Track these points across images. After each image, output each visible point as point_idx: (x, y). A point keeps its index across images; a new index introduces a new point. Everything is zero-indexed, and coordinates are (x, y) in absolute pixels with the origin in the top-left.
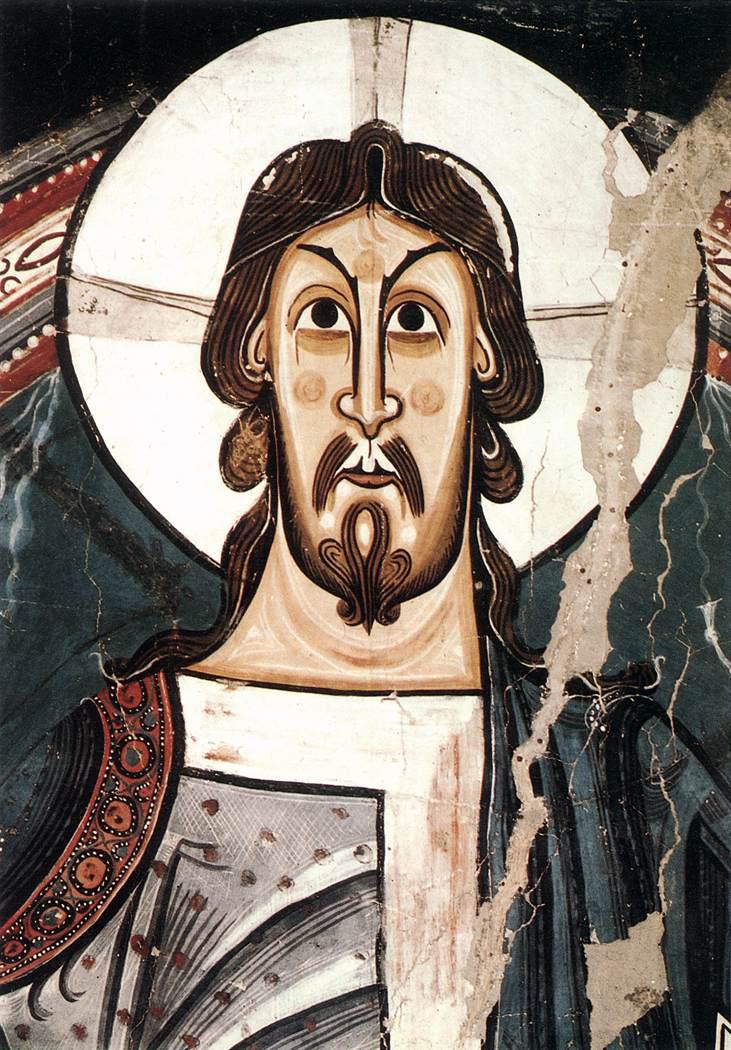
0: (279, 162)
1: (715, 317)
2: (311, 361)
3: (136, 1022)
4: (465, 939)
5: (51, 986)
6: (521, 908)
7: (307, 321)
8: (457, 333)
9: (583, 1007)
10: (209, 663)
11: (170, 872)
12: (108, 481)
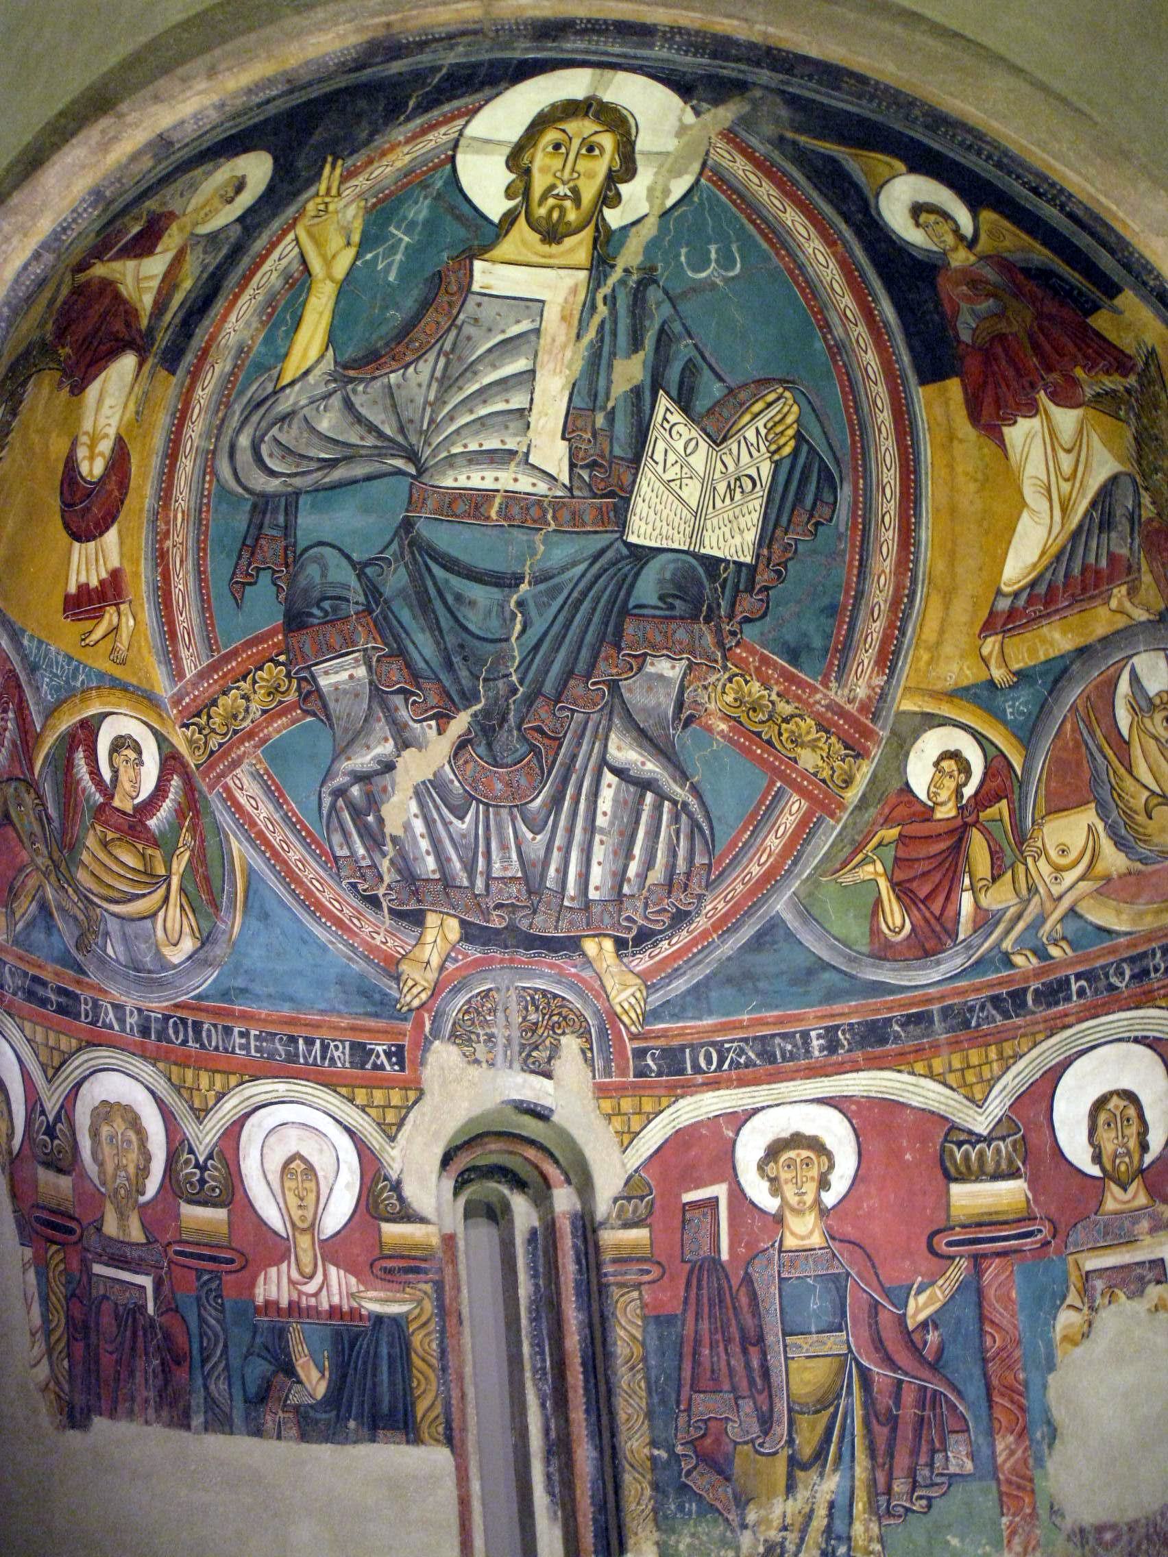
0: (553, 105)
1: (710, 162)
2: (548, 161)
3: (441, 381)
4: (568, 354)
5: (411, 369)
7: (550, 149)
8: (607, 157)
9: (610, 382)
10: (486, 256)
11: (460, 328)
12: (461, 197)
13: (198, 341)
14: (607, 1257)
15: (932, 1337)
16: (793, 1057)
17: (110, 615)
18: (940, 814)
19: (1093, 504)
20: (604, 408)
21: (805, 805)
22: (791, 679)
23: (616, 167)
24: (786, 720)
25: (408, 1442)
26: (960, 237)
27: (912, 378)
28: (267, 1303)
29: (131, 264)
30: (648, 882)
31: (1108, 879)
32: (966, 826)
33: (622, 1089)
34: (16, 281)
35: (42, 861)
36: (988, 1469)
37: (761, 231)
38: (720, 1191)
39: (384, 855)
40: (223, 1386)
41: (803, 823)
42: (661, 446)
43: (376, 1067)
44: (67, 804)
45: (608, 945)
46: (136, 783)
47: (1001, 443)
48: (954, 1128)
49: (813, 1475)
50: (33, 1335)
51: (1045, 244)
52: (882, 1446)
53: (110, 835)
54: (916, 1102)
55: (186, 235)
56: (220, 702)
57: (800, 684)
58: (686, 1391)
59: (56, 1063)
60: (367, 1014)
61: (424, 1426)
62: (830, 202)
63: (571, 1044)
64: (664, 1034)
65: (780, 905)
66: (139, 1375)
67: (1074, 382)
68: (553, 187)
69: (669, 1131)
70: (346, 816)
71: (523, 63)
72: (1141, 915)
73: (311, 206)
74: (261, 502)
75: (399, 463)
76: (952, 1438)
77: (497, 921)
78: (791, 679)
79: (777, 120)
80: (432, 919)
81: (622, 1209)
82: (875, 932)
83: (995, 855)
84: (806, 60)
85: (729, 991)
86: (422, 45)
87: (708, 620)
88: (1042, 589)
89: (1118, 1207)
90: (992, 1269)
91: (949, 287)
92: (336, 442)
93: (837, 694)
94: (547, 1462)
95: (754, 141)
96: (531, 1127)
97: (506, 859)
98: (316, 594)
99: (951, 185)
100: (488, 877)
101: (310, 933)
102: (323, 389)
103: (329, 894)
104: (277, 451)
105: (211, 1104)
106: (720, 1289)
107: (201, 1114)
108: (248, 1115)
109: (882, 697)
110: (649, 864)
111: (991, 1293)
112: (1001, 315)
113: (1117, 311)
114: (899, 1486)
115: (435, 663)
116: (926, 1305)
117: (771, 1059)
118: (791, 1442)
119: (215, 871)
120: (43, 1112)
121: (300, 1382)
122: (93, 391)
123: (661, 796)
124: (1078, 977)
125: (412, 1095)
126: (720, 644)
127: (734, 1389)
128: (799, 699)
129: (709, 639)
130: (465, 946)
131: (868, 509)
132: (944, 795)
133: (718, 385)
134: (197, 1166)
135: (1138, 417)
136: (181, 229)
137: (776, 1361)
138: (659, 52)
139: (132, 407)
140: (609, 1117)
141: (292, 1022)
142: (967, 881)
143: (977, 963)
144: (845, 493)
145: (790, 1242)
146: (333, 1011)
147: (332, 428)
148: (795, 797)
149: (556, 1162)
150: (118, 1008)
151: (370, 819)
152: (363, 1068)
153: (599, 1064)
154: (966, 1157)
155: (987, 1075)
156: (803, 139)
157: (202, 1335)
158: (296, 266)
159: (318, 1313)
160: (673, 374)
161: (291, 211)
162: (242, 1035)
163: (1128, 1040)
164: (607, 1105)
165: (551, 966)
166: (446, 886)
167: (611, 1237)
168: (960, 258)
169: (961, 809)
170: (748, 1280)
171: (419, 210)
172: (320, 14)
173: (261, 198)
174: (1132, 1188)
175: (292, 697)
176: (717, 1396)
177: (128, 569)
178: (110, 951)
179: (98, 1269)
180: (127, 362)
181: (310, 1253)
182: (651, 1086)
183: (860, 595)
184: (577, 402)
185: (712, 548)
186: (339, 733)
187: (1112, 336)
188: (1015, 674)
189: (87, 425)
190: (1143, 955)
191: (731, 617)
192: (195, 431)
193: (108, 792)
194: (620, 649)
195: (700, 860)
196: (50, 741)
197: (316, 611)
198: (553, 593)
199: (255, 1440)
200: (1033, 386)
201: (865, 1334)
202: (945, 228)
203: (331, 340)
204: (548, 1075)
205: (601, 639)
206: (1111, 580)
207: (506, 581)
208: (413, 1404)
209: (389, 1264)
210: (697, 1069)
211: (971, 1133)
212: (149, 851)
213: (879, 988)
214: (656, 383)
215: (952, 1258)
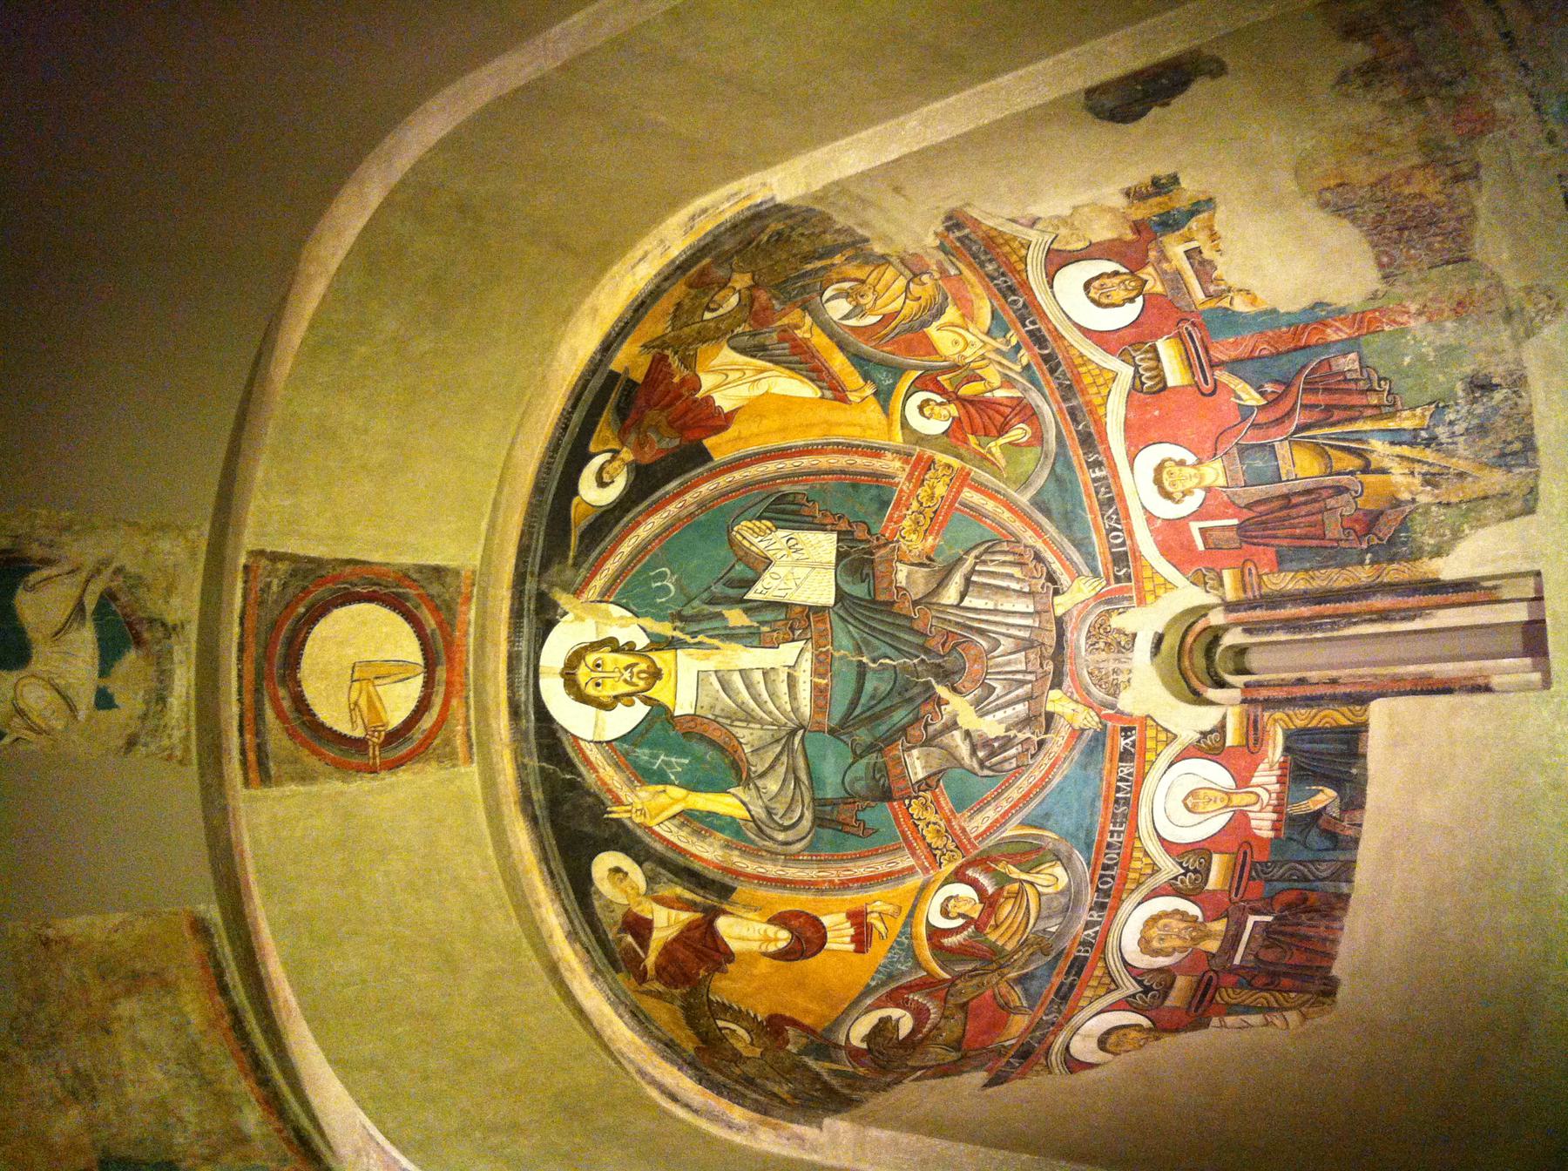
3: (749, 722)
4: (729, 652)
6: (722, 640)
9: (742, 627)
13: (715, 875)
14: (1243, 596)
15: (1269, 388)
16: (1108, 487)
17: (873, 919)
18: (955, 413)
19: (754, 356)
20: (758, 628)
21: (966, 489)
23: (609, 649)
24: (921, 504)
25: (1367, 731)
26: (613, 459)
27: (710, 465)
28: (1275, 828)
29: (655, 934)
31: (963, 316)
32: (958, 398)
33: (1140, 589)
34: (632, 1030)
35: (995, 978)
37: (639, 561)
38: (1195, 527)
40: (1323, 866)
41: (977, 490)
42: (777, 593)
44: (973, 954)
45: (1057, 599)
46: (968, 900)
47: (736, 410)
49: (1373, 458)
50: (1267, 1024)
51: (600, 415)
52: (1349, 413)
53: (992, 922)
54: (1122, 412)
56: (928, 840)
57: (899, 499)
58: (1329, 544)
59: (1107, 980)
60: (1103, 751)
61: (1355, 719)
62: (610, 530)
63: (1116, 622)
64: (1105, 565)
65: (1024, 499)
67: (683, 381)
68: (626, 681)
69: (1163, 560)
70: (994, 760)
71: (537, 720)
72: (977, 295)
73: (637, 820)
74: (818, 822)
76: (1335, 369)
77: (1050, 667)
79: (560, 572)
80: (1050, 708)
81: (1211, 588)
82: (1029, 444)
84: (517, 566)
85: (1076, 526)
86: (523, 784)
87: (872, 554)
88: (814, 375)
89: (1158, 283)
90: (1218, 355)
91: (647, 457)
92: (784, 780)
93: (901, 477)
94: (1393, 620)
95: (579, 580)
96: (1170, 642)
97: (1016, 662)
98: (872, 783)
99: (580, 471)
101: (1058, 786)
102: (753, 791)
104: (788, 815)
105: (1147, 861)
106: (1257, 523)
107: (1156, 870)
108: (1159, 836)
109: (898, 452)
110: (1011, 576)
111: (1233, 354)
112: (657, 429)
113: (627, 370)
115: (911, 708)
116: (1248, 394)
117: (1111, 500)
118: (1352, 473)
120: (1134, 996)
121: (1325, 808)
122: (735, 946)
123: (973, 571)
124: (1024, 326)
125: (1150, 722)
126: (885, 545)
127: (1321, 512)
128: (908, 499)
129: (883, 552)
130: (1065, 686)
131: (793, 475)
132: (945, 412)
133: (737, 567)
134: (1185, 874)
135: (690, 344)
136: (639, 904)
137: (1299, 486)
138: (523, 646)
139: (751, 915)
140: (1157, 597)
142: (989, 395)
143: (1033, 384)
144: (786, 488)
145: (1222, 481)
146: (1100, 773)
147: (776, 782)
149: (1194, 623)
150: (1088, 925)
151: (996, 745)
152: (1132, 754)
153: (1126, 604)
154: (1149, 378)
155: (1097, 372)
156: (571, 554)
158: (676, 821)
159: (1281, 792)
160: (731, 592)
161: (639, 832)
162: (1112, 836)
163: (1053, 293)
164: (1150, 598)
165: (1072, 634)
166: (1031, 698)
167: (1231, 596)
168: (627, 455)
169: (949, 402)
170: (1249, 506)
171: (643, 754)
172: (512, 841)
173: (627, 854)
174: (1145, 277)
175: (928, 795)
176: (1327, 522)
178: (1053, 929)
179: (1237, 961)
180: (723, 924)
181: (1244, 796)
183: (843, 472)
184: (755, 644)
185: (832, 557)
186: (948, 765)
187: (645, 369)
188: (865, 380)
189: (755, 946)
190: (1000, 290)
192: (772, 870)
193: (969, 921)
194: (894, 602)
195: (1005, 547)
196: (934, 966)
198: (867, 643)
199: (1362, 845)
200: (695, 401)
201: (1273, 430)
202: (609, 468)
203: (725, 791)
204: (1135, 635)
205: (891, 613)
206: (795, 340)
207: (862, 670)
208: (1344, 727)
209: (1251, 743)
210: (1123, 544)
211: (1134, 377)
212: (1005, 894)
214: (741, 601)
215: (1215, 381)
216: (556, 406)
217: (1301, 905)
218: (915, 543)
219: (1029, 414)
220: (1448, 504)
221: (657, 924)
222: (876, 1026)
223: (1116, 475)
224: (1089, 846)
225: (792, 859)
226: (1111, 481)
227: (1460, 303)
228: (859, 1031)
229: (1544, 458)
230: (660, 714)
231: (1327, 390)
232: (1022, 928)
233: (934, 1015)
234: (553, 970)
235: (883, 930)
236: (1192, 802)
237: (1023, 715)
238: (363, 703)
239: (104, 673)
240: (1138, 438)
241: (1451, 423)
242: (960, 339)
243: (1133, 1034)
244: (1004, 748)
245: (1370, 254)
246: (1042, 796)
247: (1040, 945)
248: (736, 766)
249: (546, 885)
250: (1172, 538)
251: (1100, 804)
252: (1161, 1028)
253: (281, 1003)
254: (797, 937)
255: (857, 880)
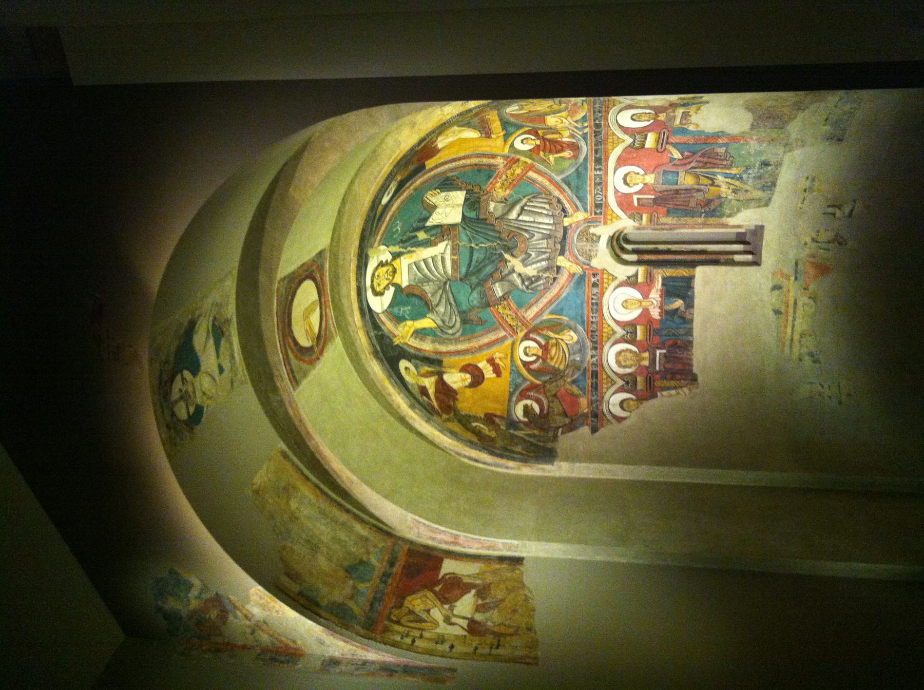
3: (428, 282)
13: (433, 356)
15: (686, 153)
17: (497, 361)
22: (497, 176)
28: (660, 315)
30: (549, 208)
36: (726, 145)
38: (635, 197)
39: (542, 275)
41: (535, 172)
43: (598, 280)
45: (566, 219)
46: (535, 348)
47: (442, 149)
48: (629, 146)
49: (716, 181)
50: (678, 394)
52: (711, 165)
54: (619, 153)
55: (418, 377)
59: (609, 380)
63: (592, 230)
64: (591, 208)
66: (681, 356)
70: (533, 285)
75: (447, 287)
77: (559, 246)
78: (497, 176)
80: (558, 264)
82: (569, 158)
83: (553, 133)
85: (581, 192)
86: (374, 346)
87: (479, 198)
90: (671, 140)
93: (502, 166)
100: (547, 248)
101: (565, 297)
103: (554, 290)
107: (614, 332)
108: (613, 318)
110: (544, 208)
114: (725, 163)
117: (600, 184)
118: (706, 185)
119: (552, 324)
120: (623, 386)
121: (679, 308)
122: (455, 386)
123: (526, 205)
124: (595, 121)
125: (605, 272)
127: (689, 197)
128: (502, 175)
129: (485, 197)
137: (684, 187)
139: (453, 370)
141: (588, 303)
142: (559, 139)
143: (584, 139)
144: (450, 174)
146: (584, 292)
148: (528, 174)
153: (598, 223)
157: (669, 335)
158: (414, 336)
159: (662, 301)
160: (421, 224)
161: (405, 347)
164: (609, 222)
165: (571, 234)
170: (661, 192)
171: (396, 310)
172: (369, 370)
175: (505, 303)
177: (485, 357)
179: (657, 368)
180: (446, 377)
182: (605, 212)
188: (503, 130)
191: (479, 193)
192: (452, 348)
193: (538, 358)
197: (484, 300)
198: (474, 238)
204: (600, 237)
205: (486, 224)
209: (648, 280)
210: (602, 200)
213: (586, 159)
214: (423, 228)
215: (665, 149)
216: (385, 169)
217: (675, 345)
218: (500, 193)
219: (575, 147)
220: (738, 200)
221: (428, 387)
222: (524, 410)
223: (606, 173)
224: (583, 322)
225: (457, 341)
226: (603, 176)
227: (772, 140)
228: (519, 412)
229: (777, 189)
230: (398, 287)
231: (709, 158)
232: (564, 360)
233: (545, 402)
234: (402, 420)
235: (503, 365)
236: (626, 304)
237: (546, 266)
238: (308, 328)
239: (218, 356)
240: (621, 162)
241: (750, 174)
242: (560, 121)
243: (631, 403)
244: (537, 280)
245: (751, 120)
246: (558, 301)
247: (575, 366)
248: (426, 303)
249: (394, 386)
250: (625, 202)
251: (585, 305)
252: (641, 399)
253: (344, 478)
254: (473, 376)
255: (485, 345)
